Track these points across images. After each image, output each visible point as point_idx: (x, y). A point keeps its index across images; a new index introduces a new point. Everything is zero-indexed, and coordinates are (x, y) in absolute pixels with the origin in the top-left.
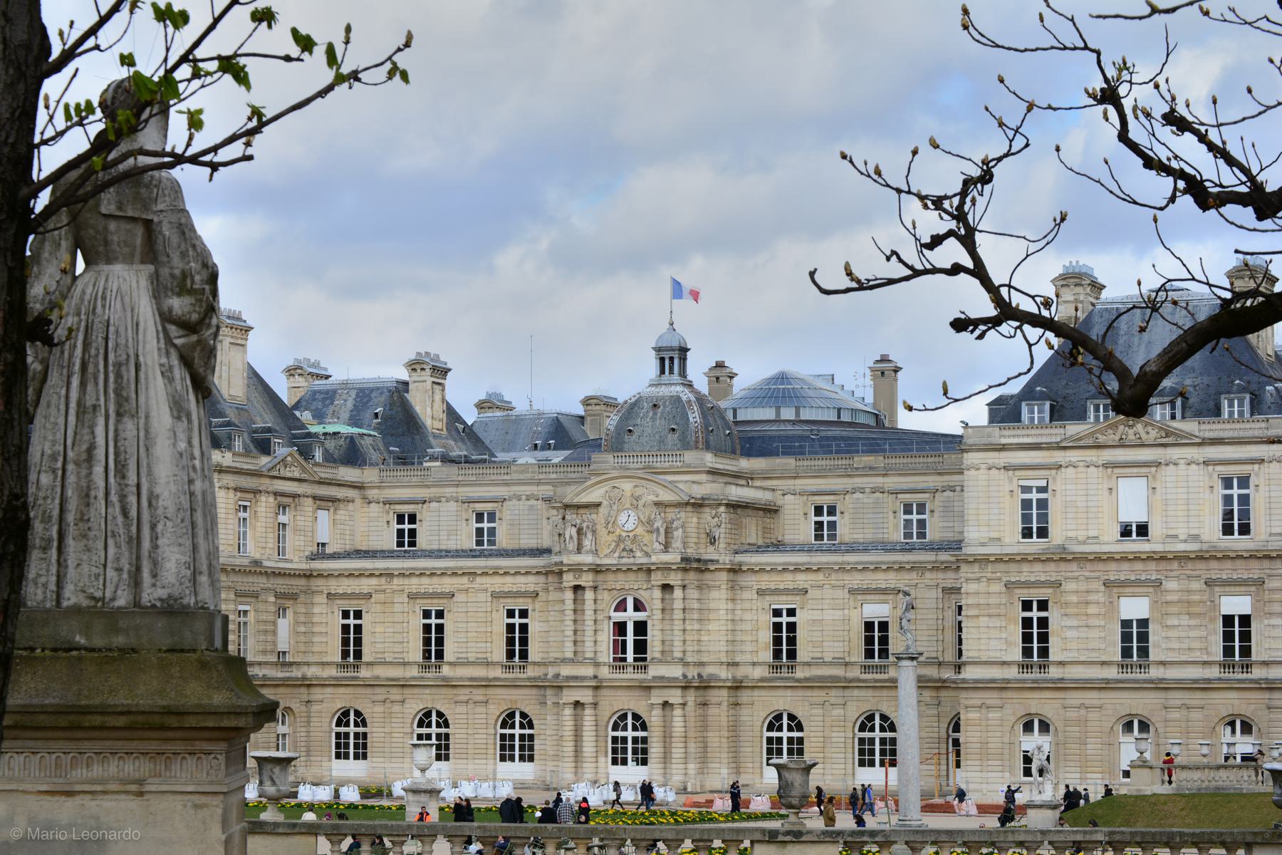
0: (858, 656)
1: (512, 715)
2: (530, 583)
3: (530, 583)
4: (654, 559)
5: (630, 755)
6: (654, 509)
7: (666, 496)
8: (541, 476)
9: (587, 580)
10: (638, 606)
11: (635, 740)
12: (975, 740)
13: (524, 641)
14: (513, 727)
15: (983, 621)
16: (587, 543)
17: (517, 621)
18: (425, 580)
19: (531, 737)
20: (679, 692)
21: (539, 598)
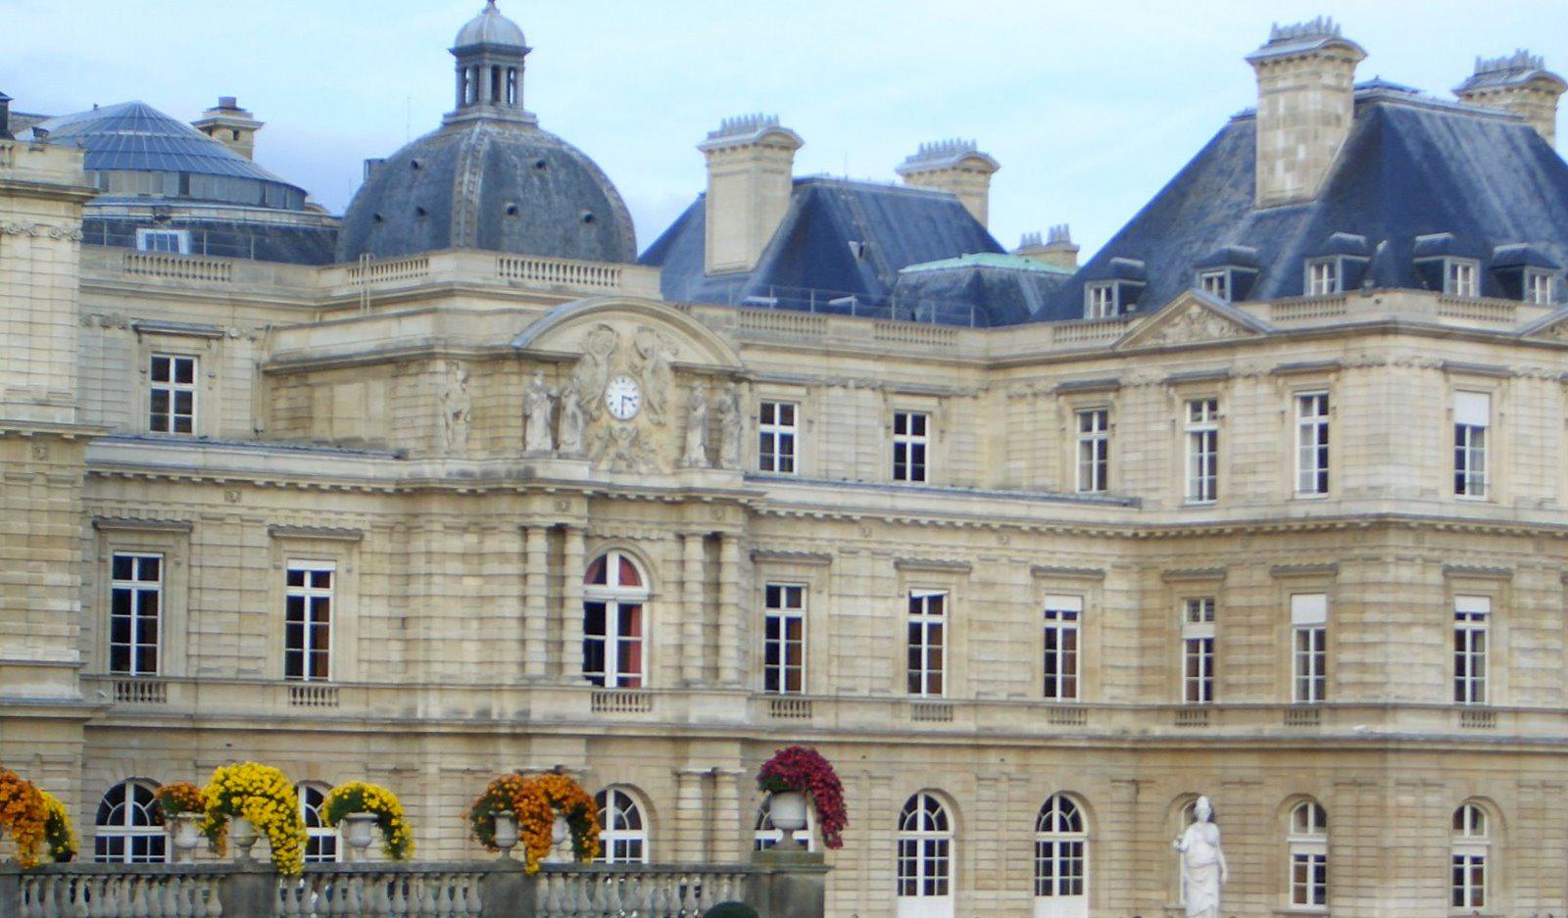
0: (901, 691)
2: (348, 512)
3: (348, 512)
4: (697, 481)
6: (668, 375)
7: (695, 355)
8: (134, 278)
9: (576, 514)
10: (629, 576)
12: (1408, 842)
13: (320, 637)
15: (1418, 633)
17: (307, 592)
18: (134, 492)
20: (735, 749)
21: (366, 547)
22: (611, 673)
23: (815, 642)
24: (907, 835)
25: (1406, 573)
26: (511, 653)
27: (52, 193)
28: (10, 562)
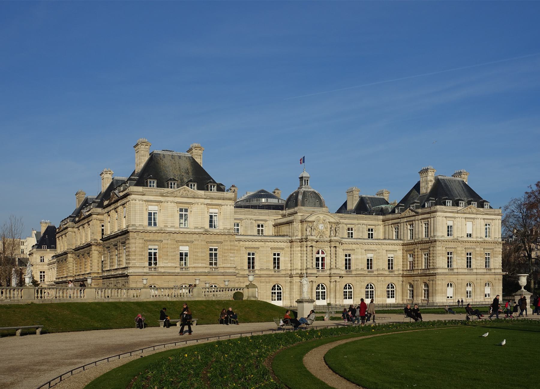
0: (366, 268)
1: (274, 286)
5: (320, 297)
7: (332, 220)
9: (314, 244)
10: (323, 253)
11: (322, 292)
14: (275, 290)
16: (313, 233)
17: (276, 257)
19: (281, 293)
22: (320, 267)
23: (352, 262)
24: (367, 290)
25: (439, 248)
26: (305, 265)
27: (230, 199)
28: (225, 253)
